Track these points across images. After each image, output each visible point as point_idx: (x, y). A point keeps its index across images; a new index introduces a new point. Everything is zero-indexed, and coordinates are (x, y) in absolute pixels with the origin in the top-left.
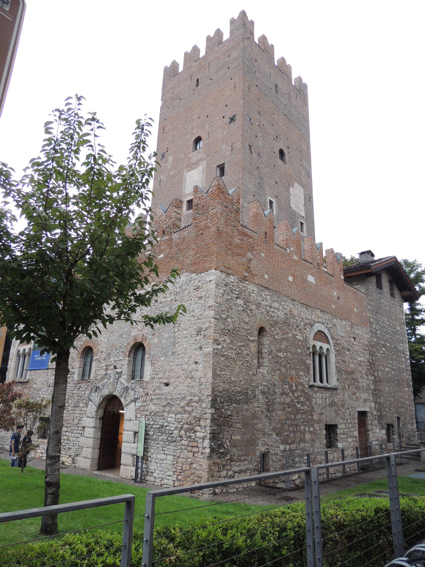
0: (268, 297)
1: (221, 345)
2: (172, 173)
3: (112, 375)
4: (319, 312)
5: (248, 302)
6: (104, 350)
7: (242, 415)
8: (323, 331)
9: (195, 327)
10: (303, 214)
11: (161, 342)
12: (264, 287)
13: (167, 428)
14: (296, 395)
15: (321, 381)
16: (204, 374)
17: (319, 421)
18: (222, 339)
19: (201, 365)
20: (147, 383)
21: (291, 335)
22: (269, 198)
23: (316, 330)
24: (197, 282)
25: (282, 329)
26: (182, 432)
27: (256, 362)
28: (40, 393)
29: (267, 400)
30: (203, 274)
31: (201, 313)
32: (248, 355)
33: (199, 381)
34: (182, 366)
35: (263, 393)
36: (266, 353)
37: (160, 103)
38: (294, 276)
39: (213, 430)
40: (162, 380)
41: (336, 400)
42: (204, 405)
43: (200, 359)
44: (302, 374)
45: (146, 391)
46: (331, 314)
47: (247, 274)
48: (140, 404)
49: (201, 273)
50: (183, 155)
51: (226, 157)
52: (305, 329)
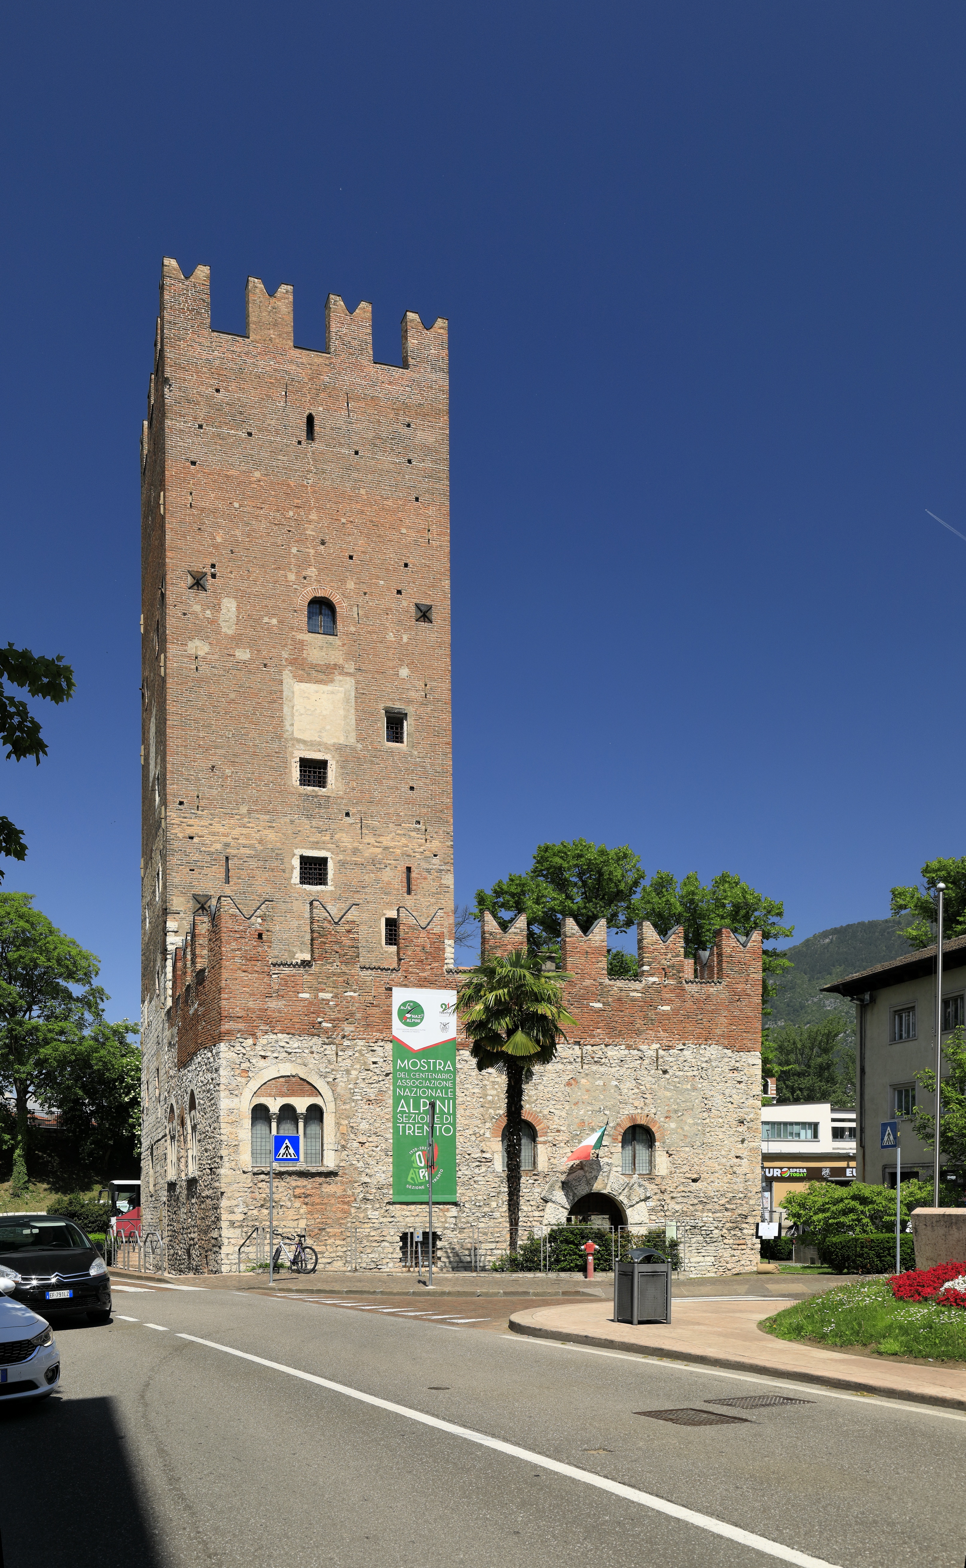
6: (562, 1128)
9: (735, 1116)
20: (663, 1178)
26: (725, 1231)
40: (689, 1176)
42: (752, 1202)
43: (744, 1154)
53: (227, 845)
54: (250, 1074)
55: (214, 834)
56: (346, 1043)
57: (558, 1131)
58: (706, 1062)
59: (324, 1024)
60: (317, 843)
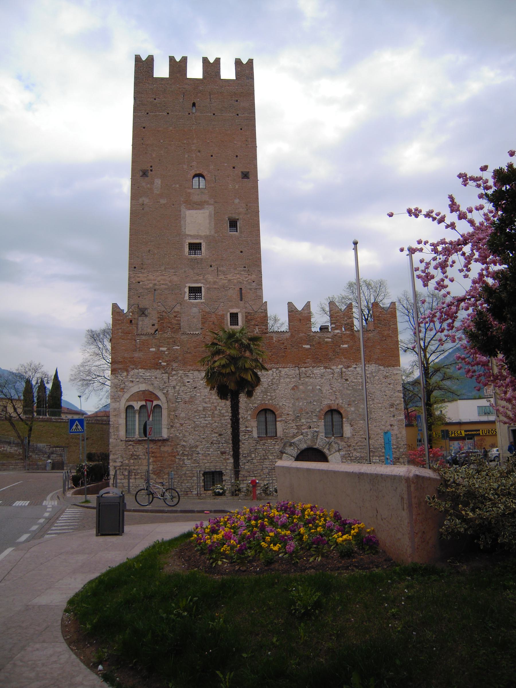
2: (163, 201)
3: (309, 433)
6: (290, 413)
11: (358, 410)
20: (348, 438)
28: (198, 450)
45: (349, 444)
48: (344, 453)
50: (178, 186)
53: (155, 284)
54: (125, 390)
55: (149, 280)
56: (174, 373)
57: (288, 415)
58: (370, 373)
59: (163, 364)
60: (197, 280)
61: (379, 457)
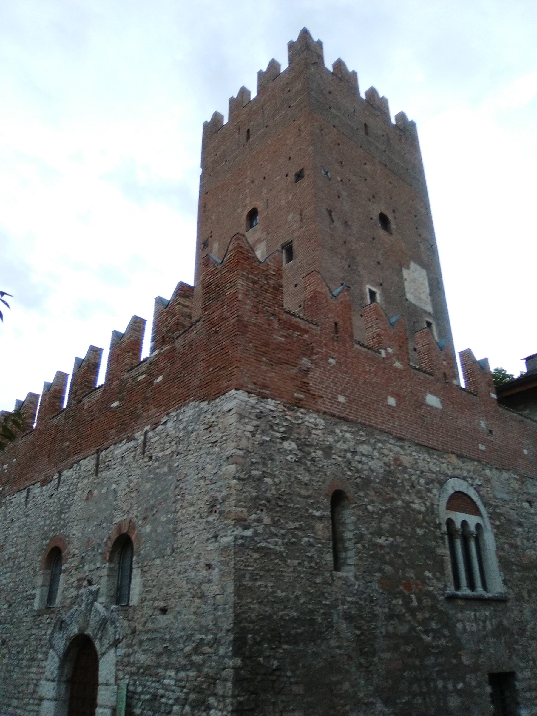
0: (348, 435)
1: (252, 530)
4: (454, 459)
5: (307, 446)
6: (77, 551)
7: (304, 667)
8: (465, 491)
9: (206, 498)
10: (429, 308)
12: (339, 418)
13: (163, 700)
14: (420, 616)
15: (472, 586)
16: (220, 587)
17: (475, 668)
18: (254, 516)
19: (217, 570)
20: (135, 609)
21: (399, 503)
22: (368, 287)
23: (451, 492)
24: (209, 416)
25: (381, 493)
27: (329, 557)
29: (359, 632)
30: (217, 400)
31: (215, 471)
32: (311, 545)
33: (212, 602)
34: (187, 574)
35: (348, 617)
36: (350, 540)
37: (200, 171)
38: (397, 396)
39: (240, 703)
40: (157, 604)
41: (506, 623)
44: (430, 575)
46: (479, 461)
47: (301, 396)
48: (123, 651)
49: (215, 399)
51: (294, 232)
52: (429, 491)
61: (178, 671)
